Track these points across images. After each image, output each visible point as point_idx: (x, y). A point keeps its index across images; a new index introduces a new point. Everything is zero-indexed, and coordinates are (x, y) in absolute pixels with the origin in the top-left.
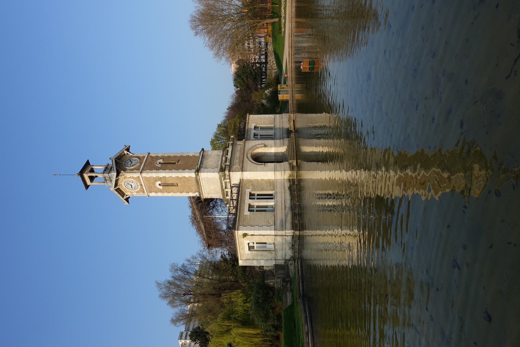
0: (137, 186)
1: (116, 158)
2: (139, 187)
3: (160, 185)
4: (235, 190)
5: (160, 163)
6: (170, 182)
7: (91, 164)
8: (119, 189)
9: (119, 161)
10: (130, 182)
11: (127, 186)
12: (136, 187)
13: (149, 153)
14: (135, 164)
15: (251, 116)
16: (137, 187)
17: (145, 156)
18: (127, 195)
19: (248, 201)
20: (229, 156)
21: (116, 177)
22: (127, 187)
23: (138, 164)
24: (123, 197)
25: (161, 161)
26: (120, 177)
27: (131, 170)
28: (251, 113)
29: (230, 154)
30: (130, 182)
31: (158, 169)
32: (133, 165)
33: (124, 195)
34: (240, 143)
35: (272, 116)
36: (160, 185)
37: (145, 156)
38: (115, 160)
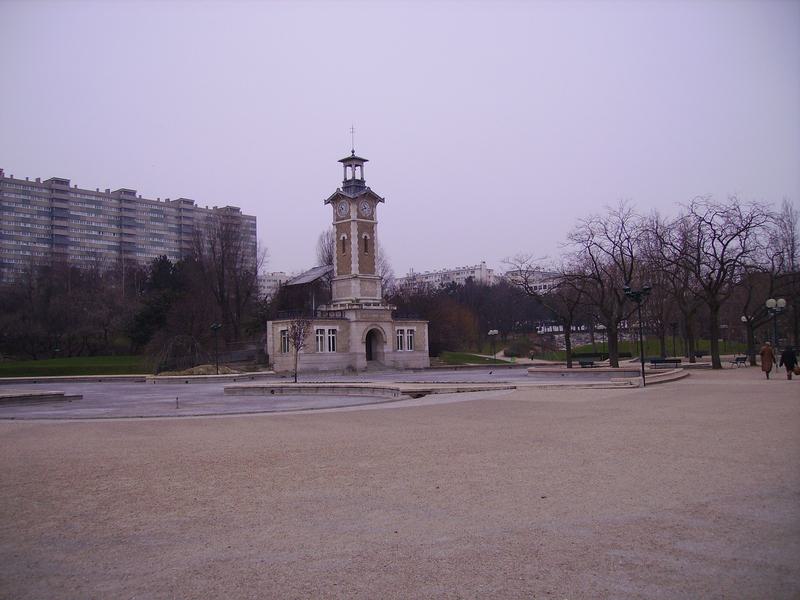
4: (339, 315)
6: (347, 248)
15: (427, 326)
19: (326, 328)
20: (372, 307)
25: (368, 238)
28: (428, 324)
29: (375, 307)
31: (359, 236)
34: (388, 317)
35: (427, 348)
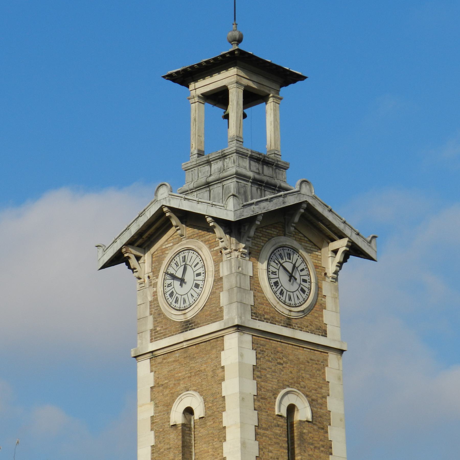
0: (181, 305)
1: (310, 209)
2: (178, 317)
3: (189, 411)
5: (291, 409)
7: (284, 90)
8: (167, 225)
9: (296, 219)
10: (198, 275)
11: (179, 259)
12: (176, 301)
13: (341, 351)
14: (282, 293)
16: (178, 306)
17: (324, 335)
18: (138, 258)
21: (217, 220)
22: (177, 259)
23: (283, 309)
24: (131, 243)
26: (219, 231)
27: (254, 280)
30: (198, 275)
32: (276, 284)
33: (140, 246)
36: (189, 411)
37: (324, 335)
38: (297, 206)
